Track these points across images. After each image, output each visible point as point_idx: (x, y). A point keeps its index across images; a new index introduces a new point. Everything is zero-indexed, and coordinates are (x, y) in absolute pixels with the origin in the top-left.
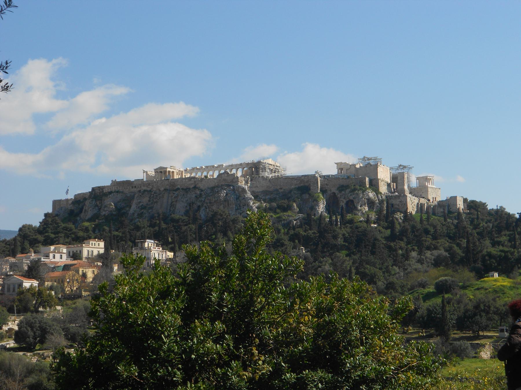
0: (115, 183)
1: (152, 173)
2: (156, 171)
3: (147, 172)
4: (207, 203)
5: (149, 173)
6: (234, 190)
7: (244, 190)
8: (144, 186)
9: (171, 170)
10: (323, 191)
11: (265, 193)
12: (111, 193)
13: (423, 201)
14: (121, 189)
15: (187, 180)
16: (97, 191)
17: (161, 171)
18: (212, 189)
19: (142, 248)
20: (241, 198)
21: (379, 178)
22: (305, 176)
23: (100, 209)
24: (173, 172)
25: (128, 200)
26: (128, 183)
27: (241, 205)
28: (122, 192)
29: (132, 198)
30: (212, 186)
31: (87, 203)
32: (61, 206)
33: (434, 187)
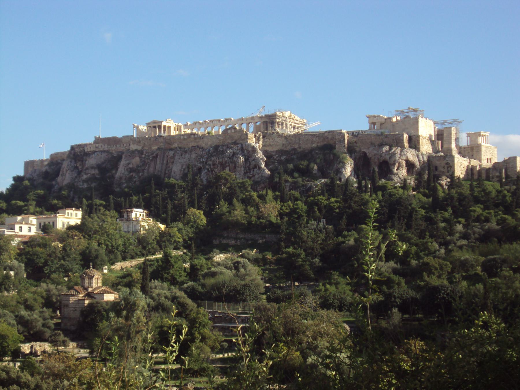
1: (143, 128)
2: (148, 124)
3: (137, 127)
4: (210, 165)
7: (254, 149)
9: (167, 125)
10: (351, 150)
11: (281, 152)
13: (474, 162)
14: (106, 147)
16: (77, 150)
17: (155, 126)
18: (216, 148)
19: (129, 219)
20: (251, 159)
21: (420, 134)
22: (329, 132)
24: (169, 127)
25: (115, 160)
27: (251, 166)
29: (119, 158)
31: (65, 165)
32: (36, 168)
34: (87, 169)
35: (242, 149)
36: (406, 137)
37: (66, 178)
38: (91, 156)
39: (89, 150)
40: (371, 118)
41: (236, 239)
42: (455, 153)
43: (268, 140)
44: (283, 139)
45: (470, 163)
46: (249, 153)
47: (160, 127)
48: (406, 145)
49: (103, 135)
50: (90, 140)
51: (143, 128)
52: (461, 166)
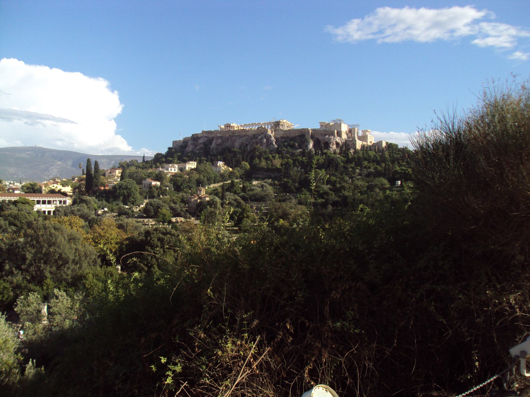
1: (223, 127)
7: (270, 136)
10: (312, 137)
13: (365, 143)
14: (207, 135)
17: (228, 126)
18: (254, 135)
19: (216, 166)
25: (210, 141)
29: (212, 140)
31: (189, 143)
35: (265, 136)
36: (336, 131)
37: (190, 148)
41: (262, 175)
42: (356, 139)
46: (268, 138)
47: (230, 126)
48: (336, 135)
49: (206, 130)
50: (201, 132)
51: (223, 127)
52: (359, 144)
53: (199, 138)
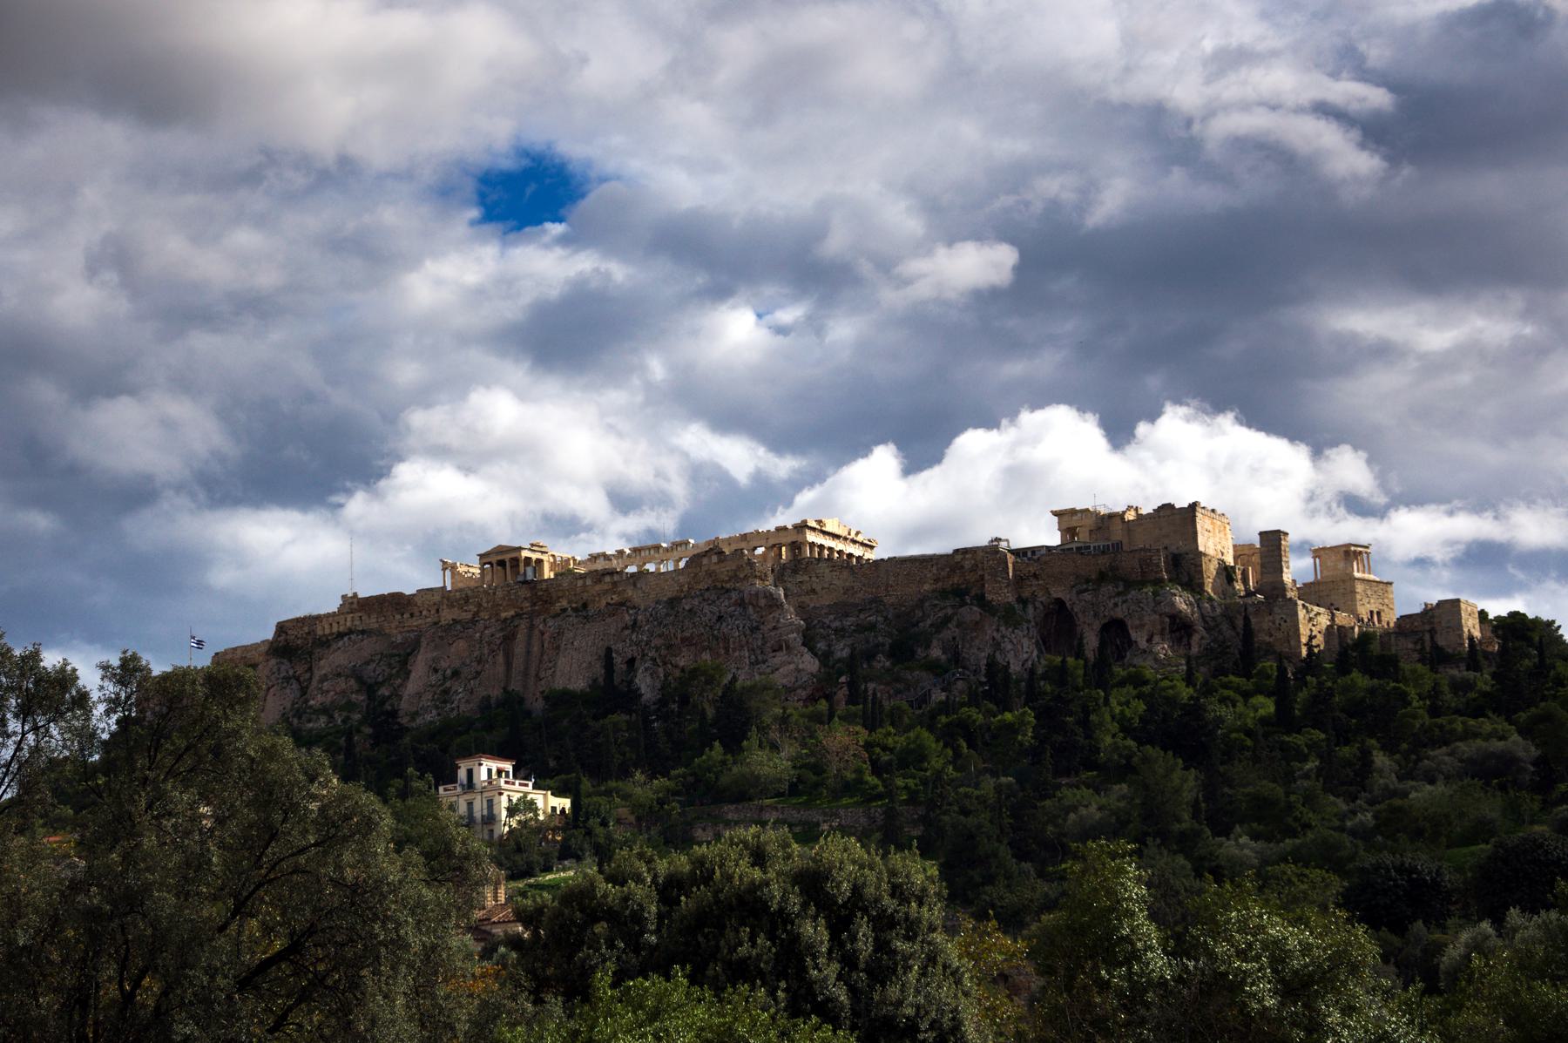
0: (354, 605)
3: (453, 567)
4: (657, 649)
5: (461, 569)
6: (741, 603)
8: (451, 606)
9: (534, 556)
11: (842, 609)
12: (340, 635)
13: (1343, 618)
14: (372, 622)
15: (589, 582)
18: (673, 602)
19: (470, 784)
20: (765, 628)
21: (1201, 549)
22: (965, 551)
23: (304, 691)
24: (539, 561)
26: (395, 603)
28: (379, 633)
29: (412, 647)
30: (669, 595)
33: (1372, 577)
34: (324, 679)
38: (334, 646)
39: (327, 631)
40: (1066, 518)
43: (806, 578)
44: (846, 573)
45: (1332, 620)
47: (515, 561)
50: (332, 605)
52: (1312, 624)
53: (325, 643)
